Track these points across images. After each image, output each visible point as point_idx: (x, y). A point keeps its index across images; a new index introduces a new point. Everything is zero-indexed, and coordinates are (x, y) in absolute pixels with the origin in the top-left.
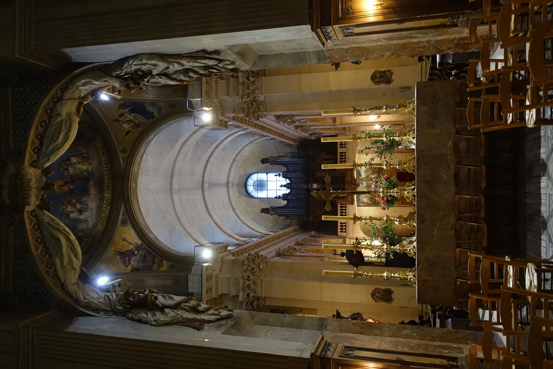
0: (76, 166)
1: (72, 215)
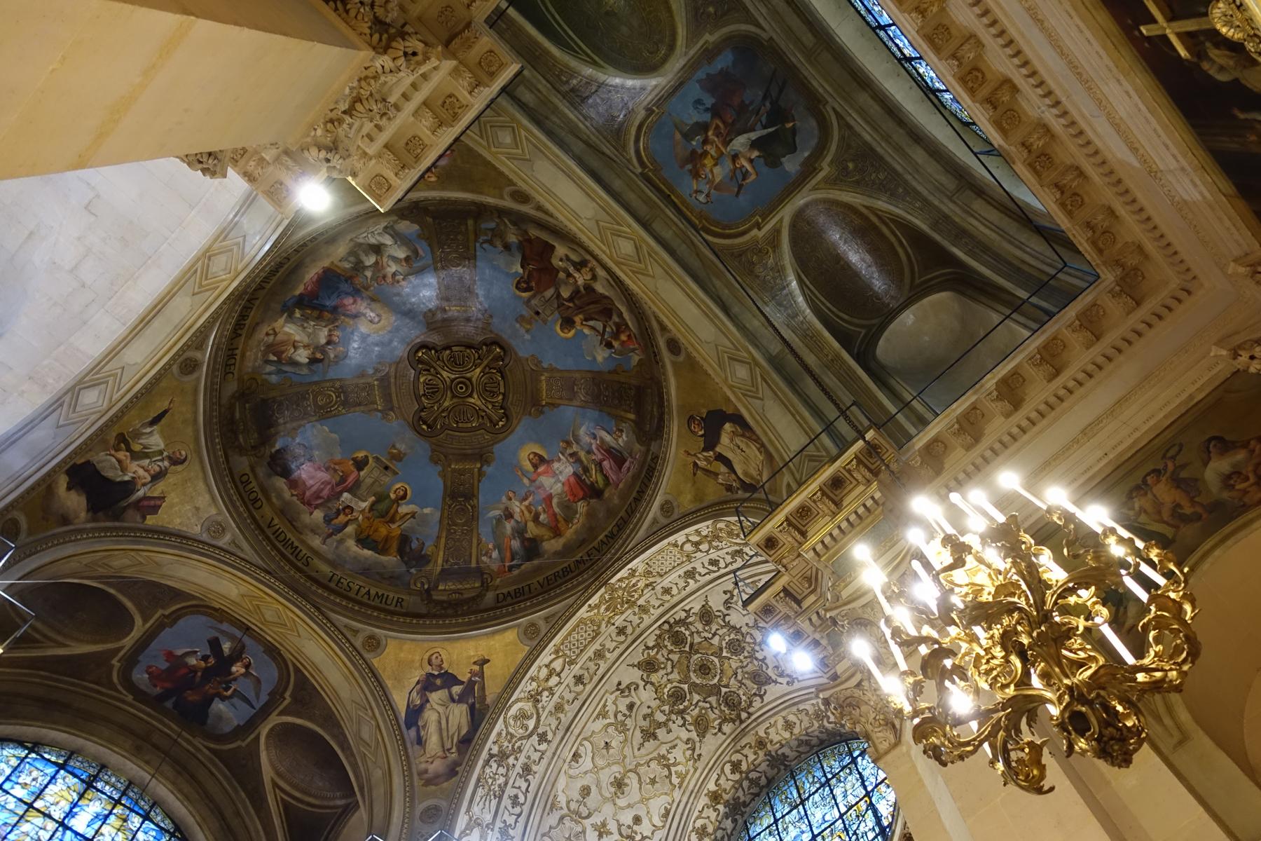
0: (306, 340)
1: (401, 254)
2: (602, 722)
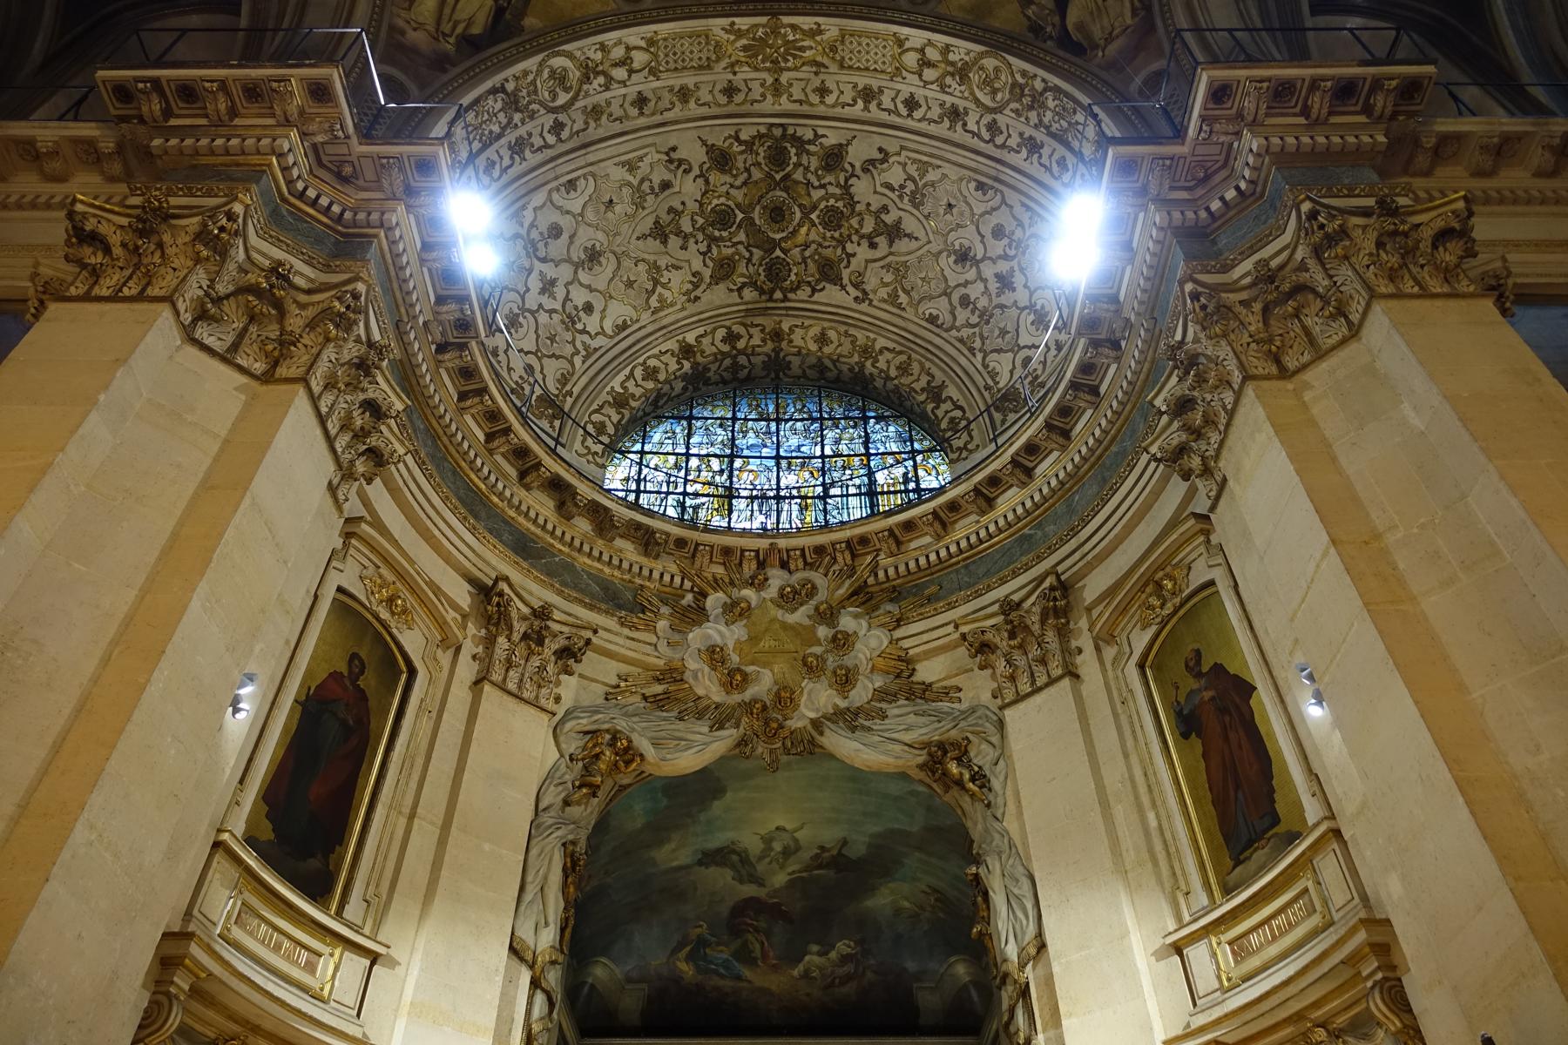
2: (619, 174)
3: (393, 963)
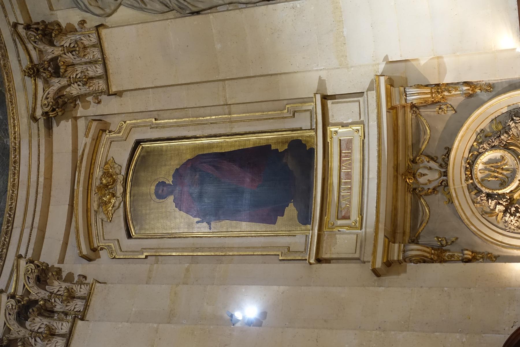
3: (322, 83)
